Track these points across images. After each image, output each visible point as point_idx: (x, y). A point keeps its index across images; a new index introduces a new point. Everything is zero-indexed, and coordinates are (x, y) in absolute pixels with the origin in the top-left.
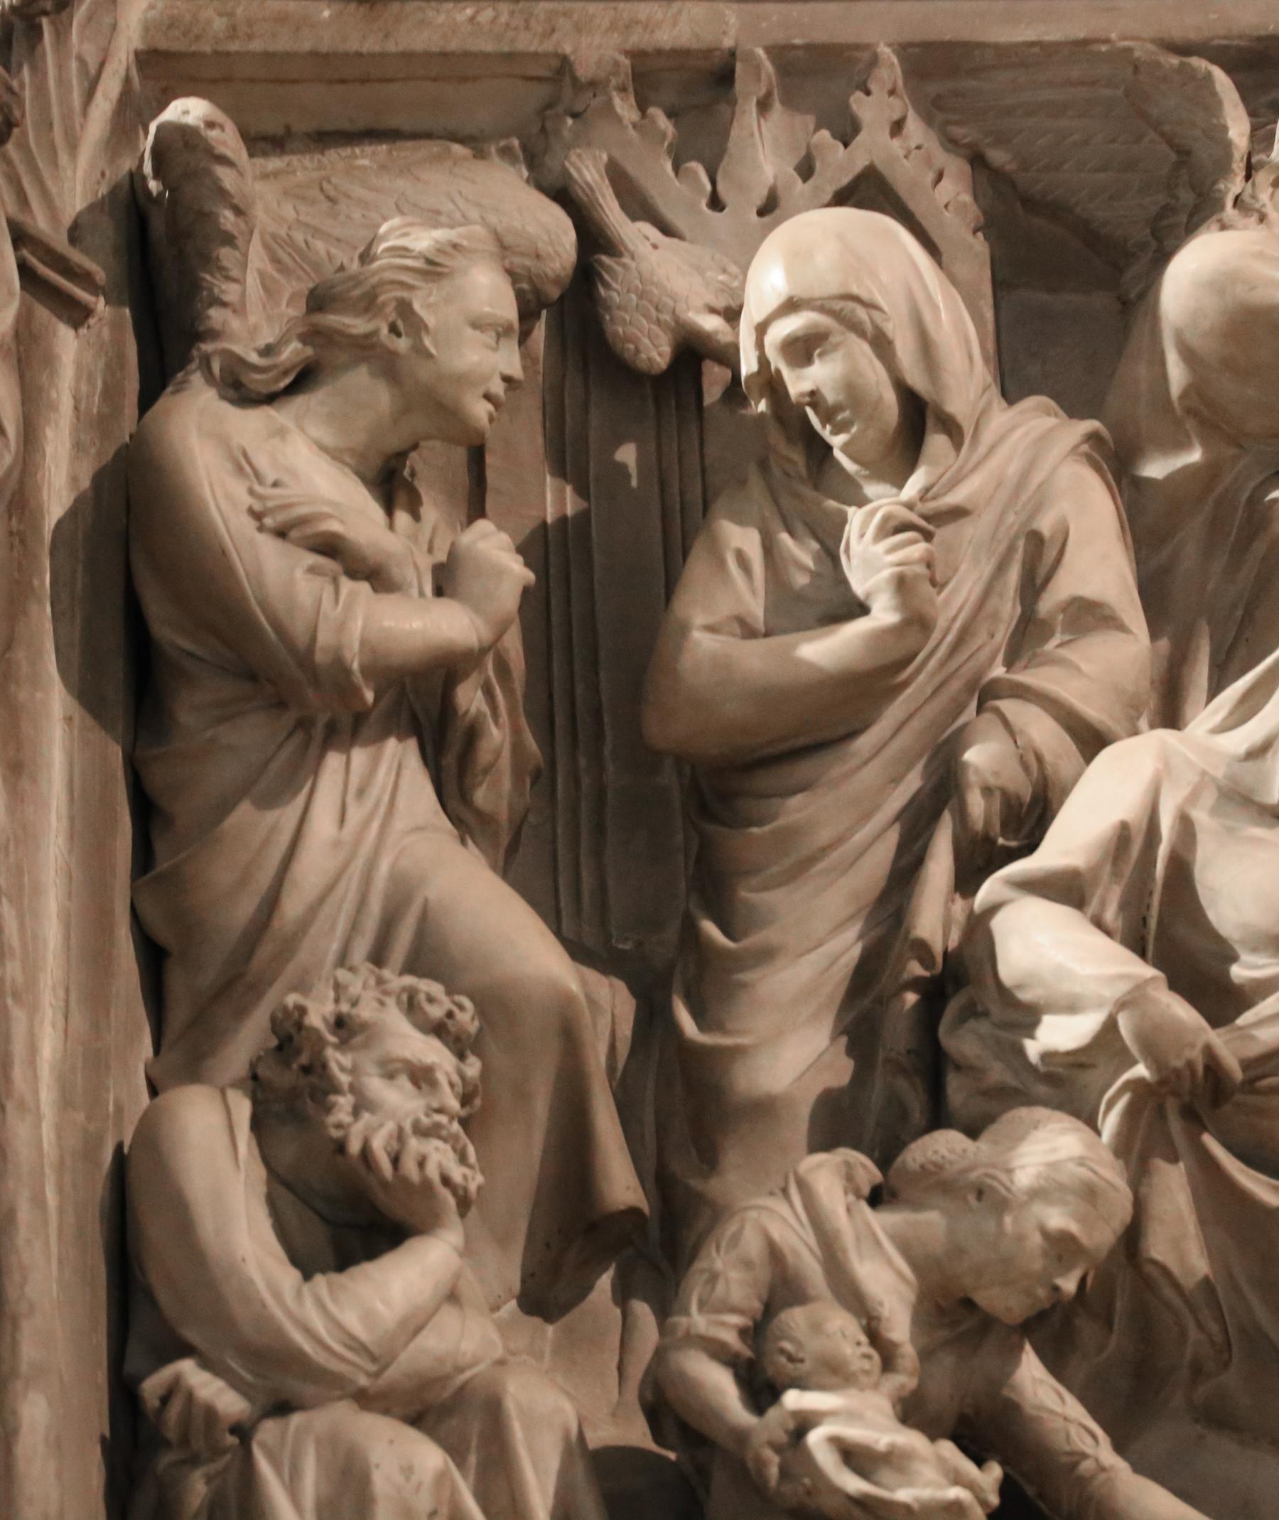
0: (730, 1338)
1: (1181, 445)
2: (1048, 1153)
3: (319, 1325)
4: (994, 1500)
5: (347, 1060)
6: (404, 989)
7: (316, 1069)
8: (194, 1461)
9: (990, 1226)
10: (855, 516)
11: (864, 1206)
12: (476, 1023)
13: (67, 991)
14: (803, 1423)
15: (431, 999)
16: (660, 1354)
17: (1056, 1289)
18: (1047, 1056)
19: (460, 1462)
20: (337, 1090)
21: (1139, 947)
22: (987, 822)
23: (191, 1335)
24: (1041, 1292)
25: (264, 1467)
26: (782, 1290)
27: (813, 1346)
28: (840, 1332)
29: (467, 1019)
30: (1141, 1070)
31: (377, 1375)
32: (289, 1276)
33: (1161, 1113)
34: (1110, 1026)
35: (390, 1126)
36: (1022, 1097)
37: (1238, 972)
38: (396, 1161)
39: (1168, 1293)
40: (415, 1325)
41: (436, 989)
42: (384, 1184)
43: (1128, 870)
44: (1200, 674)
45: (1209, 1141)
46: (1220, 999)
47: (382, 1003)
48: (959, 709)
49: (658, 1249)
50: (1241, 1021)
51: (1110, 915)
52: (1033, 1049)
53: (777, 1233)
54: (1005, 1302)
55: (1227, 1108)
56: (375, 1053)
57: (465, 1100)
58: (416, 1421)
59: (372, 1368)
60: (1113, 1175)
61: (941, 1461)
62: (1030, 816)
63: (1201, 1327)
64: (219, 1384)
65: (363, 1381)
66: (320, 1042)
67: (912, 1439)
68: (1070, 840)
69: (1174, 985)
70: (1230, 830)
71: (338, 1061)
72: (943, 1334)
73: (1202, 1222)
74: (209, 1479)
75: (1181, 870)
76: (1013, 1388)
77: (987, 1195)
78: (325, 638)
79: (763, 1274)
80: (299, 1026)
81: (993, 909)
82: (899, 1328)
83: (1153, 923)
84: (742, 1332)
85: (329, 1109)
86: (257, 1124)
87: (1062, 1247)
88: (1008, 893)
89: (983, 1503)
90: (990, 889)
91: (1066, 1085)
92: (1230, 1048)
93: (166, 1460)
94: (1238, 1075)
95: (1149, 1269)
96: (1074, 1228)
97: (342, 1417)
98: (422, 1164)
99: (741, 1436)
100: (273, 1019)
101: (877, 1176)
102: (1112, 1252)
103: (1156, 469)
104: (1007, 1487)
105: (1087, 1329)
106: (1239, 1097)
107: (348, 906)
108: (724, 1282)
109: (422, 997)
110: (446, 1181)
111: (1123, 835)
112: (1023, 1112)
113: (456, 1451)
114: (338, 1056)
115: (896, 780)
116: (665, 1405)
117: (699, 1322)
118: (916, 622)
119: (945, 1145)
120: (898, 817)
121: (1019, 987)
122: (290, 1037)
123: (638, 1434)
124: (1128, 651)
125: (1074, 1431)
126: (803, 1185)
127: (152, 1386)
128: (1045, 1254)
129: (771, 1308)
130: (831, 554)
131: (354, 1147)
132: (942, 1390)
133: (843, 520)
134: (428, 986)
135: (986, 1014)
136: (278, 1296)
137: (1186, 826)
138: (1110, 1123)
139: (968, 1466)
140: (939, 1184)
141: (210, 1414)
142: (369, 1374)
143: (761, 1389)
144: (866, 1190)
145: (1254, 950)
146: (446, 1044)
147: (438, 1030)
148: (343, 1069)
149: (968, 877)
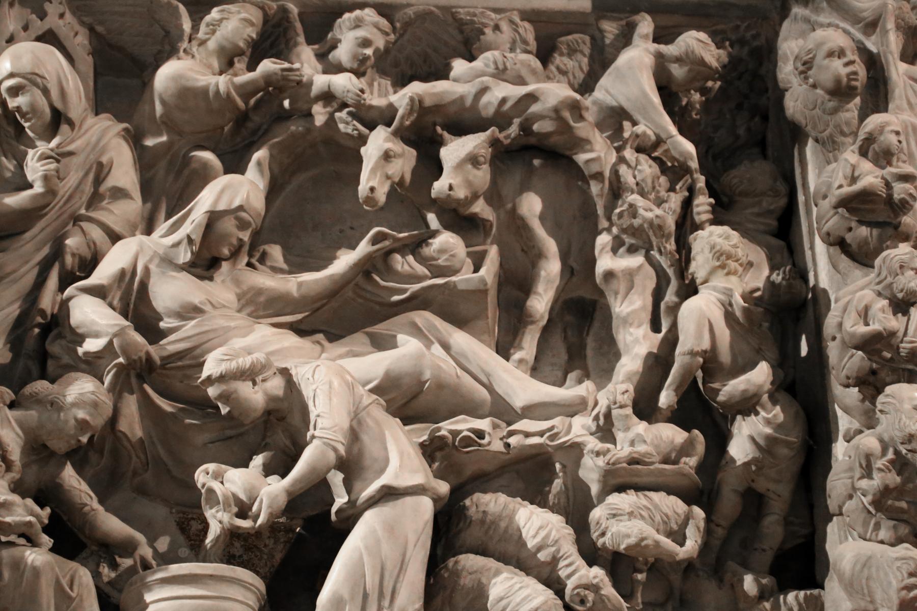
1: (160, 134)
2: (80, 389)
4: (46, 521)
9: (56, 416)
10: (31, 152)
11: (6, 408)
17: (79, 441)
18: (86, 353)
21: (125, 314)
22: (73, 267)
24: (73, 442)
30: (121, 360)
33: (128, 375)
34: (110, 343)
36: (75, 369)
37: (162, 324)
39: (126, 443)
43: (124, 286)
44: (162, 215)
45: (147, 388)
46: (154, 334)
48: (67, 224)
50: (161, 343)
54: (59, 446)
55: (153, 375)
60: (107, 401)
61: (26, 506)
62: (89, 264)
63: (138, 457)
67: (16, 498)
68: (102, 274)
69: (137, 329)
70: (163, 273)
72: (34, 458)
73: (142, 417)
75: (144, 286)
76: (61, 479)
77: (55, 405)
81: (70, 299)
83: (132, 306)
87: (83, 425)
88: (76, 293)
89: (41, 522)
90: (69, 291)
91: (92, 365)
94: (159, 362)
95: (119, 434)
96: (88, 418)
101: (13, 397)
102: (104, 427)
103: (150, 142)
104: (51, 517)
105: (93, 457)
106: (159, 371)
111: (123, 273)
112: (73, 374)
115: (38, 250)
118: (50, 192)
119: (41, 386)
120: (39, 264)
121: (78, 327)
124: (134, 206)
125: (83, 495)
128: (76, 428)
130: (20, 166)
133: (26, 154)
135: (65, 337)
137: (147, 270)
138: (108, 379)
139: (37, 509)
140: (37, 401)
144: (8, 402)
145: (169, 317)
149: (62, 288)
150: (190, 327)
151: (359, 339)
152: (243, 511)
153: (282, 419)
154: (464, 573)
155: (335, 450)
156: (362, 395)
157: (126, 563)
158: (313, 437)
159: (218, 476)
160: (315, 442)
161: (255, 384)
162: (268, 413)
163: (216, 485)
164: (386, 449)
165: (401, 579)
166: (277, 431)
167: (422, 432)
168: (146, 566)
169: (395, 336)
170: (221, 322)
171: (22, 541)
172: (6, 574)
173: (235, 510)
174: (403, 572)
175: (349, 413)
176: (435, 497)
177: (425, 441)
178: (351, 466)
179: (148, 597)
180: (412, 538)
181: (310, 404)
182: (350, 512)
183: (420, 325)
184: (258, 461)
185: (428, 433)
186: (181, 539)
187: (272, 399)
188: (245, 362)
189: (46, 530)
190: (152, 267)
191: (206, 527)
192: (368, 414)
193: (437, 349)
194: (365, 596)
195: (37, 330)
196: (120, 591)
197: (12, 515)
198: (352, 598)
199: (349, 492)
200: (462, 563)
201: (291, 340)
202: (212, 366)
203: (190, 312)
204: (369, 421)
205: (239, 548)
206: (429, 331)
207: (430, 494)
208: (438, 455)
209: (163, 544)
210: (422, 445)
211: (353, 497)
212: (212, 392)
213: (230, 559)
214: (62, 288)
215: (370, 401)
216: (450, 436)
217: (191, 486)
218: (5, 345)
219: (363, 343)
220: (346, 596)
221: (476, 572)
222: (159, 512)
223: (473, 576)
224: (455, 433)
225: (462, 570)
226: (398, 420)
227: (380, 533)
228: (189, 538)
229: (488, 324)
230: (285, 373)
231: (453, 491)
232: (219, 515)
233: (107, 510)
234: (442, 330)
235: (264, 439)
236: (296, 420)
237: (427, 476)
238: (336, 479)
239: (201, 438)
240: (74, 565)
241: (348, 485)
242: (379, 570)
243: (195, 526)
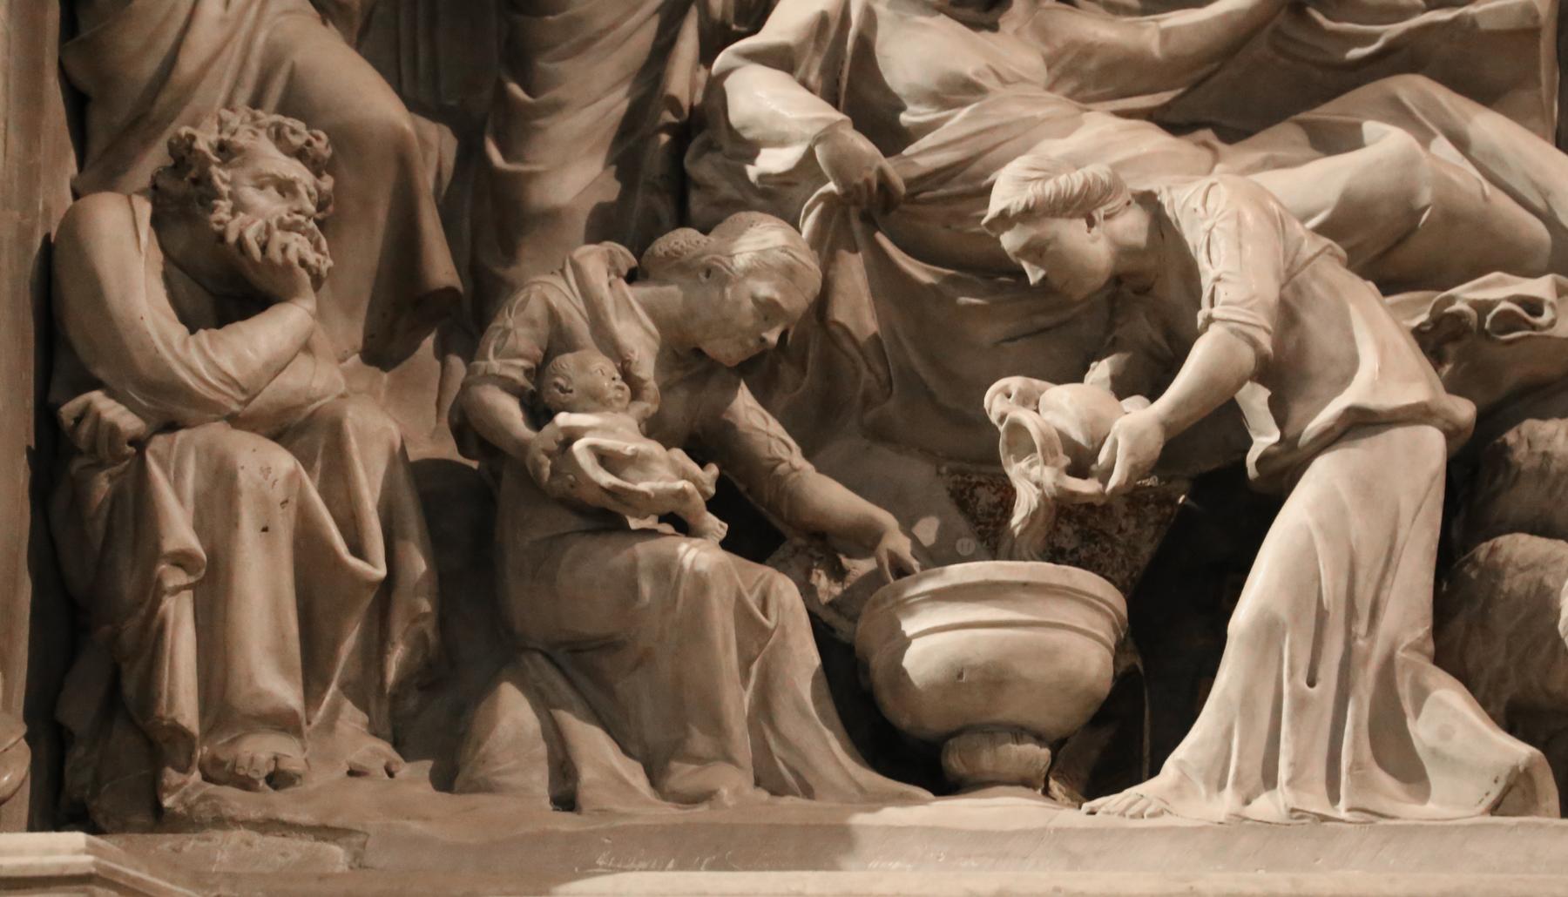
0: (518, 376)
2: (760, 245)
4: (712, 490)
5: (227, 175)
6: (273, 124)
9: (716, 294)
11: (623, 282)
12: (330, 150)
13: (6, 123)
14: (571, 436)
15: (294, 132)
16: (465, 387)
17: (763, 340)
18: (763, 177)
19: (309, 467)
20: (219, 196)
21: (833, 99)
24: (751, 343)
26: (558, 340)
27: (580, 380)
28: (602, 371)
29: (322, 146)
30: (831, 186)
31: (246, 403)
33: (845, 217)
34: (810, 155)
35: (260, 222)
36: (744, 206)
37: (905, 118)
38: (264, 248)
39: (847, 345)
40: (277, 367)
41: (299, 125)
42: (254, 263)
46: (892, 137)
47: (255, 134)
49: (465, 318)
50: (906, 152)
51: (813, 78)
52: (752, 172)
53: (555, 300)
54: (725, 350)
55: (894, 214)
56: (249, 170)
57: (321, 207)
58: (277, 437)
59: (242, 398)
60: (809, 262)
61: (673, 463)
63: (870, 369)
65: (235, 408)
66: (206, 161)
67: (653, 447)
69: (858, 126)
71: (219, 175)
72: (678, 374)
73: (874, 295)
76: (730, 413)
77: (714, 273)
79: (544, 330)
80: (190, 149)
81: (725, 74)
82: (646, 369)
83: (844, 84)
84: (527, 372)
85: (213, 210)
86: (156, 221)
87: (768, 310)
88: (737, 61)
89: (704, 493)
90: (722, 60)
91: (777, 197)
92: (897, 171)
94: (903, 189)
95: (833, 328)
96: (777, 296)
97: (217, 433)
98: (284, 249)
99: (523, 446)
100: (170, 144)
101: (634, 262)
102: (806, 315)
104: (721, 482)
105: (787, 372)
106: (903, 207)
108: (514, 338)
109: (287, 130)
110: (303, 263)
112: (743, 215)
113: (306, 461)
114: (221, 171)
116: (468, 426)
117: (494, 364)
119: (684, 239)
121: (744, 128)
122: (183, 157)
123: (448, 450)
125: (774, 443)
126: (576, 267)
128: (755, 315)
129: (549, 354)
131: (232, 237)
132: (678, 410)
134: (289, 122)
135: (720, 149)
138: (808, 224)
139: (694, 467)
140: (680, 266)
142: (240, 403)
143: (539, 413)
144: (625, 272)
145: (918, 102)
146: (306, 165)
147: (300, 154)
148: (224, 181)
150: (959, 121)
151: (1287, 134)
152: (1081, 462)
153: (1144, 291)
154: (1510, 570)
155: (1254, 343)
156: (1301, 240)
157: (861, 567)
158: (1210, 320)
159: (1029, 400)
160: (1215, 330)
161: (1091, 223)
162: (1117, 279)
163: (1026, 417)
164: (1351, 339)
165: (1388, 582)
166: (1137, 312)
167: (1419, 308)
168: (901, 570)
169: (1358, 126)
170: (1017, 110)
171: (667, 528)
172: (646, 587)
173: (1066, 461)
174: (1392, 567)
175: (1277, 275)
176: (1449, 427)
177: (1422, 324)
178: (1284, 372)
179: (909, 627)
180: (1407, 505)
181: (1201, 258)
182: (1286, 460)
183: (1406, 101)
184: (1101, 370)
185: (1429, 308)
186: (960, 523)
187: (1125, 252)
188: (1072, 181)
189: (713, 505)
190: (881, 9)
191: (1007, 494)
192: (1314, 275)
193: (1443, 148)
194: (1321, 617)
195: (665, 138)
196: (854, 619)
197: (648, 479)
198: (1296, 618)
199: (1281, 423)
200: (1505, 551)
201: (1154, 140)
202: (1006, 193)
203: (956, 91)
204: (1317, 288)
205: (1074, 531)
206: (1425, 113)
207: (1439, 421)
208: (1451, 350)
209: (928, 530)
210: (1418, 333)
211: (1290, 432)
212: (1010, 241)
213: (1055, 555)
214: (707, 54)
215: (1316, 249)
216: (1473, 313)
217: (980, 423)
218: (606, 166)
219: (1295, 143)
220: (1284, 614)
221: (1532, 566)
222: (917, 473)
223: (1528, 575)
224: (1483, 307)
225: (1506, 564)
226: (1371, 284)
227: (1345, 497)
228: (973, 518)
229: (1540, 97)
230: (1148, 200)
231: (1482, 417)
232: (1036, 472)
233: (819, 470)
234: (1451, 110)
235: (1111, 326)
236: (1172, 291)
237: (1433, 388)
238: (1255, 399)
239: (988, 332)
240: (765, 571)
241: (1279, 409)
242: (1346, 565)
243: (986, 497)
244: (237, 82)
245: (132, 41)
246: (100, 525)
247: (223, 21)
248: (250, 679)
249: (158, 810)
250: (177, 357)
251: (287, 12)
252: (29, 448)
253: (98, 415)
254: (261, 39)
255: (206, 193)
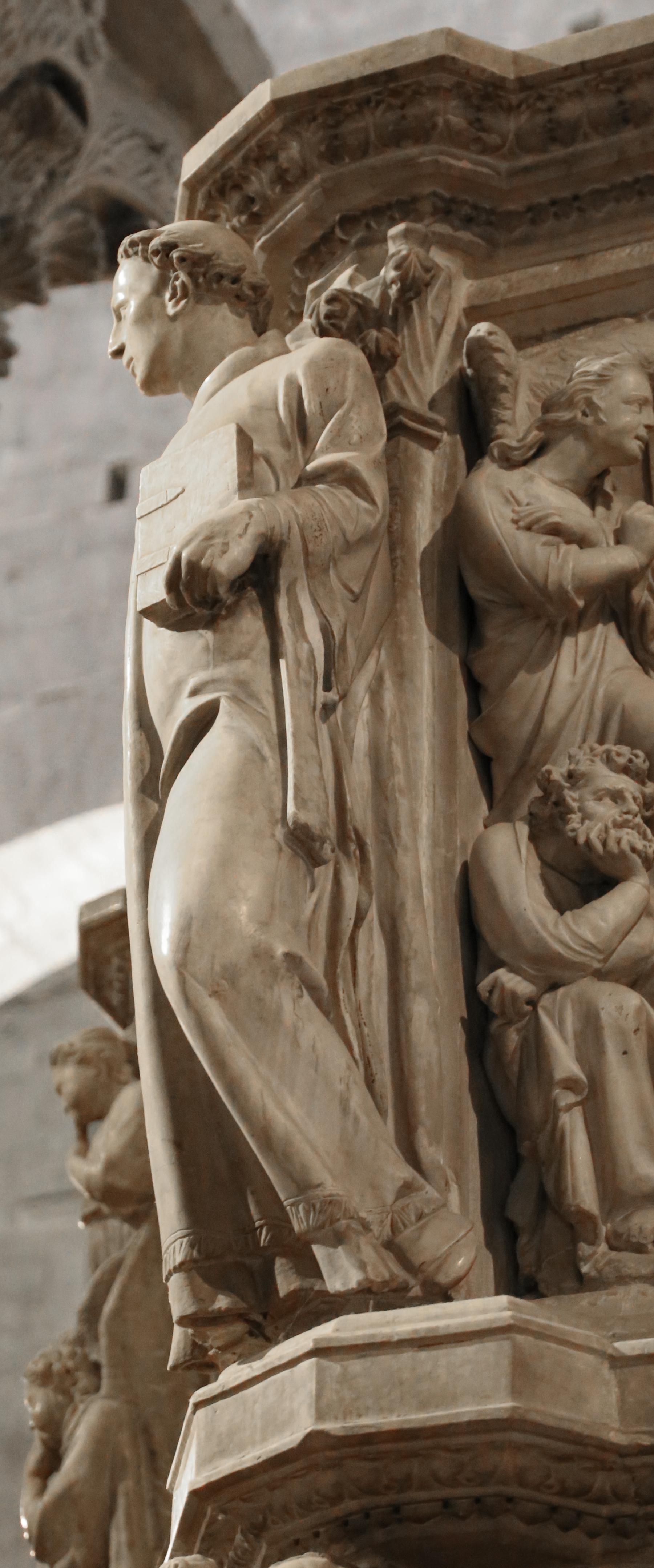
3: (566, 937)
5: (575, 795)
6: (604, 752)
7: (560, 802)
8: (510, 1023)
12: (647, 764)
13: (434, 787)
15: (619, 755)
20: (571, 811)
23: (503, 955)
25: (545, 1019)
31: (605, 960)
32: (551, 915)
35: (600, 825)
38: (604, 844)
42: (600, 857)
47: (592, 761)
58: (633, 985)
59: (601, 957)
64: (518, 978)
65: (596, 965)
66: (561, 788)
71: (571, 796)
74: (519, 1031)
78: (553, 577)
80: (549, 781)
85: (566, 822)
86: (533, 838)
93: (495, 1025)
97: (589, 986)
98: (619, 842)
107: (583, 718)
109: (613, 754)
110: (634, 850)
114: (571, 793)
127: (484, 985)
131: (581, 840)
136: (544, 925)
141: (514, 995)
142: (599, 961)
146: (632, 778)
147: (625, 770)
148: (574, 800)
244: (587, 729)
245: (513, 712)
246: (515, 1068)
247: (572, 684)
248: (632, 1167)
249: (580, 1277)
250: (551, 935)
251: (617, 669)
252: (462, 1019)
253: (503, 988)
254: (601, 692)
255: (561, 809)
